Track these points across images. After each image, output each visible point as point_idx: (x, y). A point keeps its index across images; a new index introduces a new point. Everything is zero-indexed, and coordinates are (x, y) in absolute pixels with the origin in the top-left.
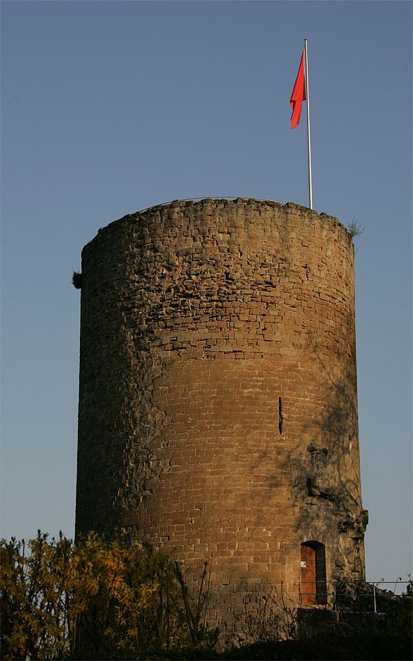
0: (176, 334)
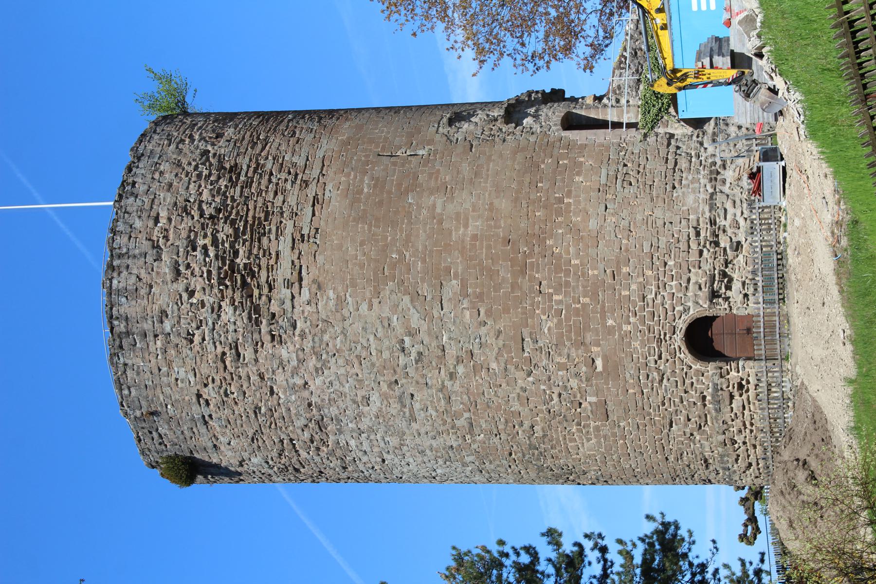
0: (280, 280)
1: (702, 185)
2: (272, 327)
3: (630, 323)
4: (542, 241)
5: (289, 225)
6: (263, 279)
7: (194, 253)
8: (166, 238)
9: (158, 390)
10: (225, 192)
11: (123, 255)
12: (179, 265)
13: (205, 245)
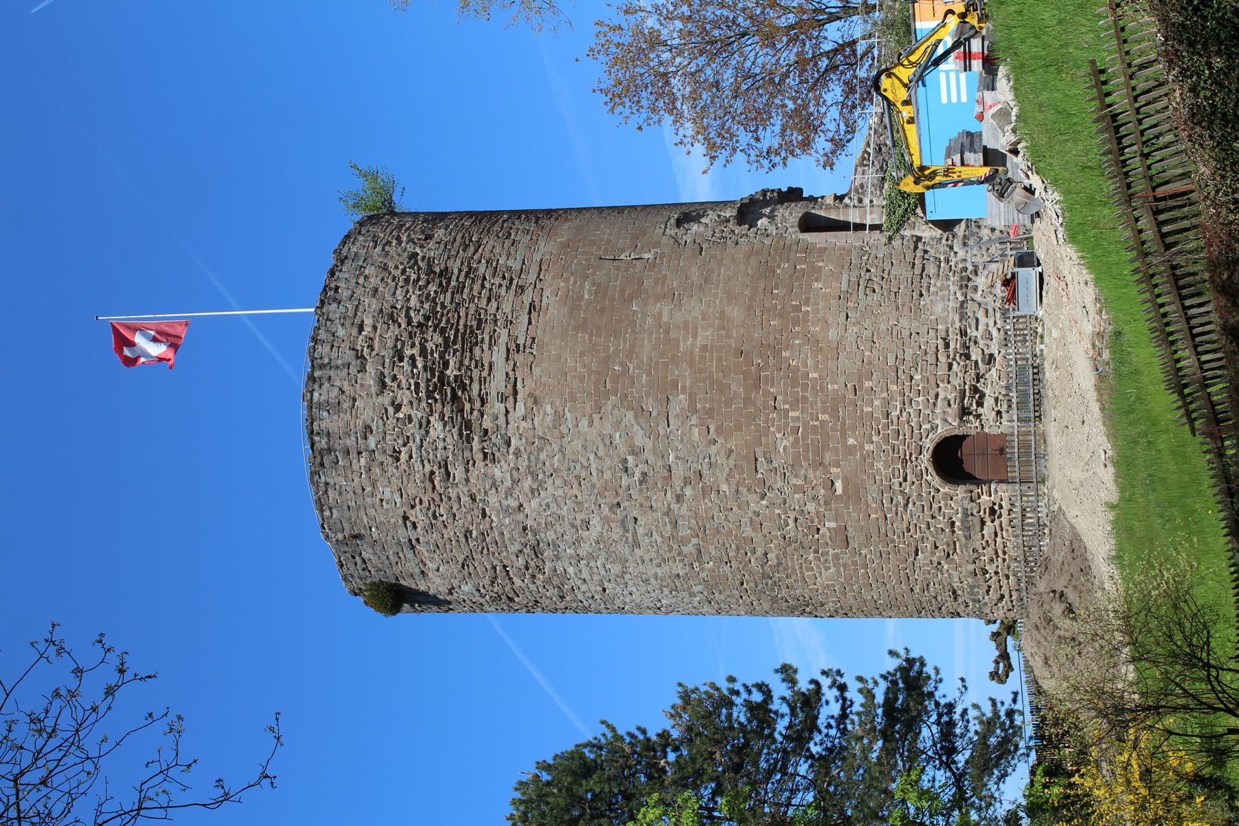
0: (493, 393)
1: (952, 292)
2: (485, 444)
3: (872, 443)
4: (777, 353)
7: (401, 364)
8: (371, 347)
9: (362, 512)
10: (434, 299)
12: (385, 377)
13: (413, 355)
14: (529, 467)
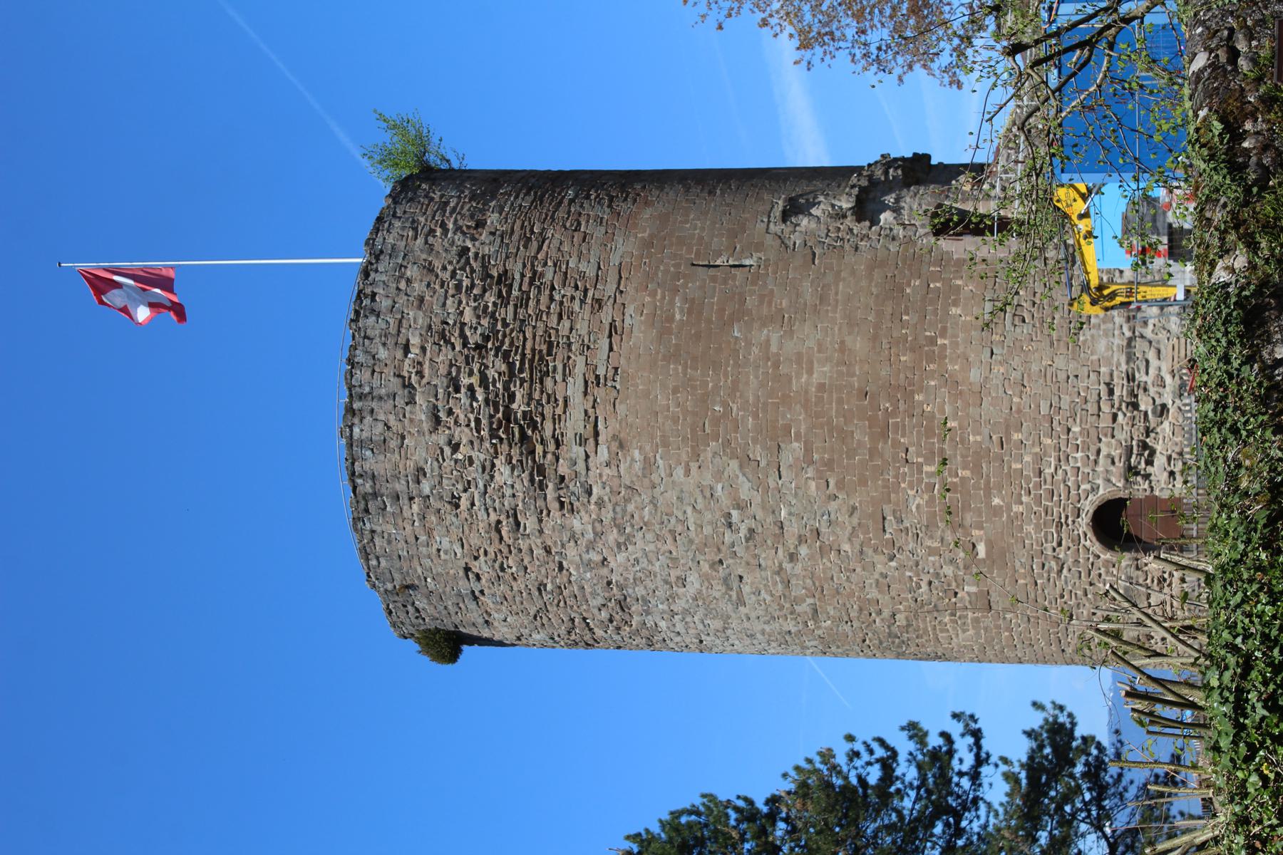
0: (570, 434)
2: (561, 492)
3: (1022, 503)
5: (580, 361)
6: (548, 433)
7: (458, 395)
8: (420, 374)
9: (415, 563)
10: (493, 313)
11: (366, 396)
12: (438, 411)
13: (471, 385)
14: (614, 519)
